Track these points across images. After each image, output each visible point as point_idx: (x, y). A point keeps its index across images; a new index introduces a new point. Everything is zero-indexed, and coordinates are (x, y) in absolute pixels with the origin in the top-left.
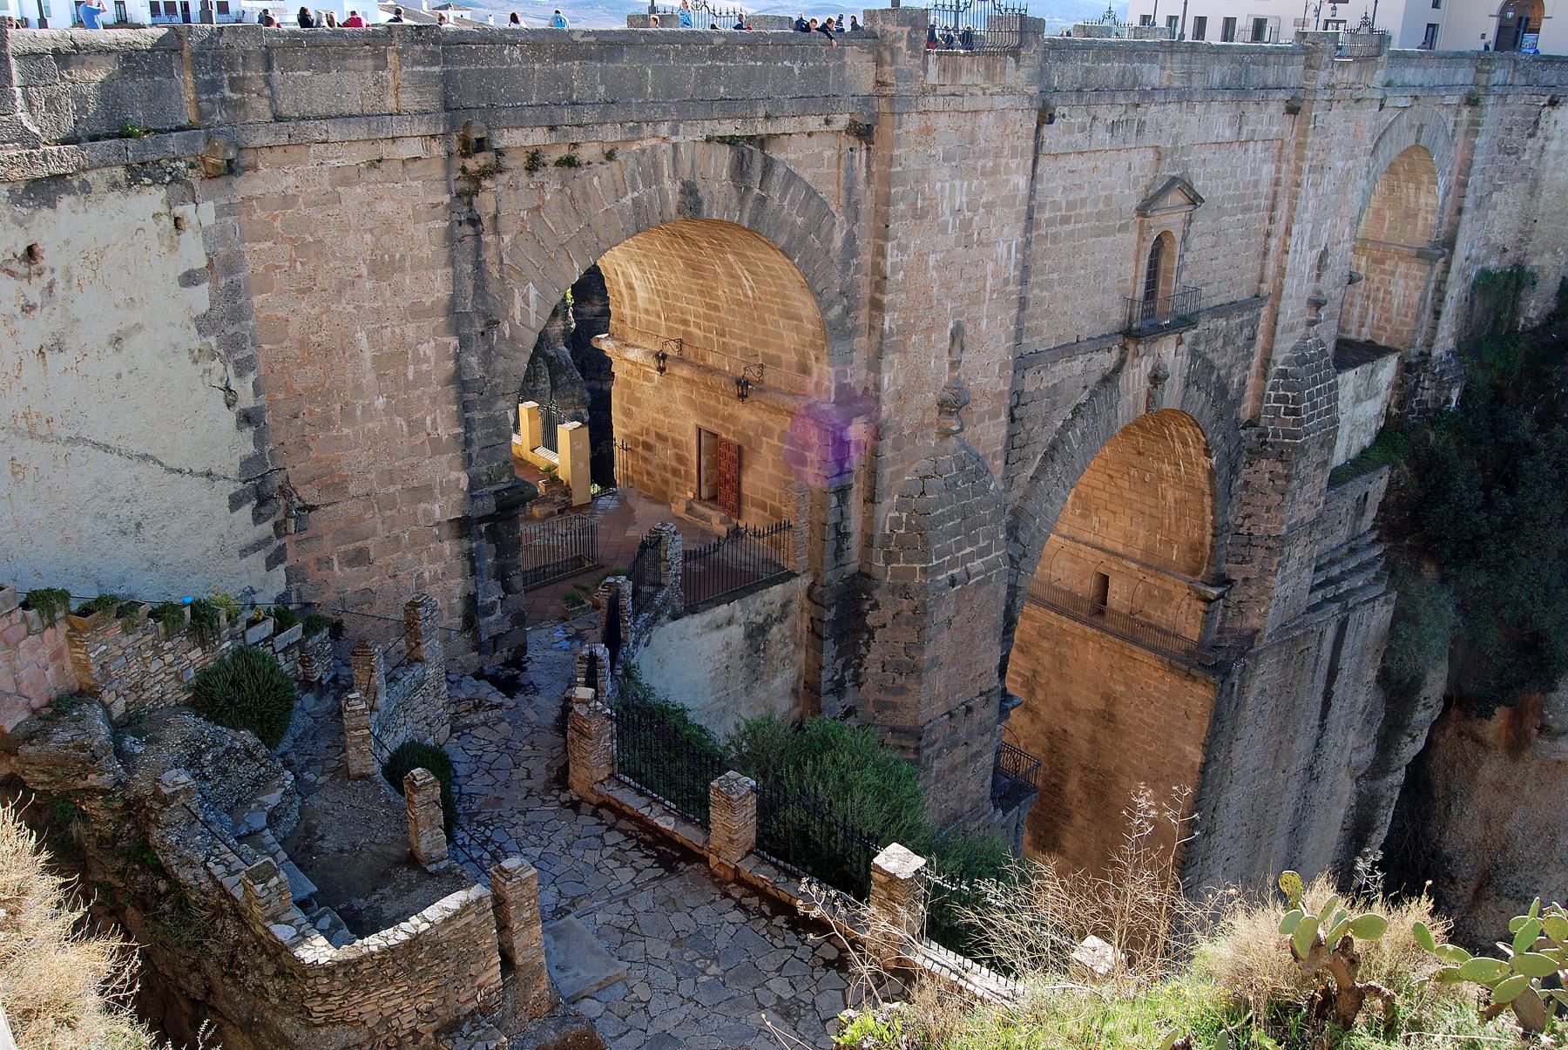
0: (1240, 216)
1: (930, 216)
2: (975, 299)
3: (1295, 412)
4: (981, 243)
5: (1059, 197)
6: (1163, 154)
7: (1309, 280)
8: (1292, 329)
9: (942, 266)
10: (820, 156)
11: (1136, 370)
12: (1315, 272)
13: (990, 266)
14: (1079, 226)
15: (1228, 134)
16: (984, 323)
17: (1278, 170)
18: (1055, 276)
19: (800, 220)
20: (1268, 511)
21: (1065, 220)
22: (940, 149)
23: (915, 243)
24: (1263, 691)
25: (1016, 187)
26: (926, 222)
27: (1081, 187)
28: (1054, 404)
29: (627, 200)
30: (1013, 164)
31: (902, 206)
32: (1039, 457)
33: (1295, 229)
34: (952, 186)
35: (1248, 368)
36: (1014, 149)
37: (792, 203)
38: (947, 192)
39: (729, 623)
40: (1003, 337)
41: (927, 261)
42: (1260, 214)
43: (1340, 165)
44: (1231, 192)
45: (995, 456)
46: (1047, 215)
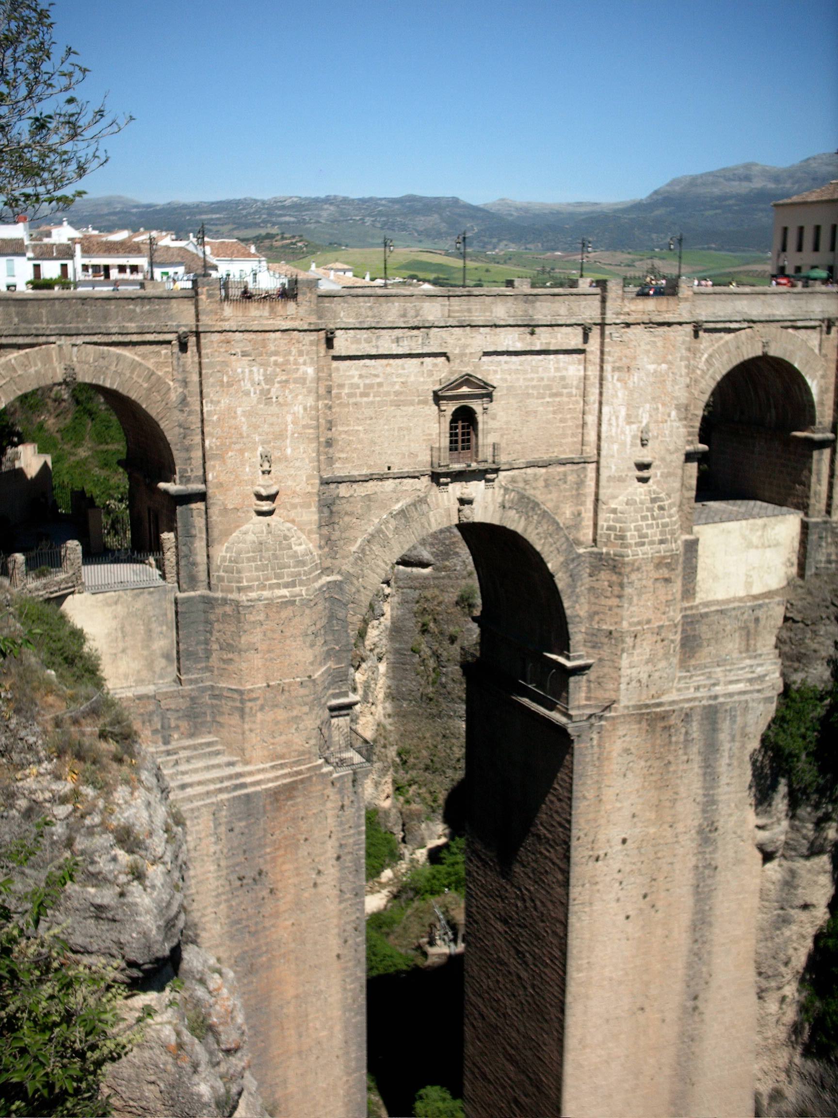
0: (548, 399)
1: (235, 387)
2: (280, 436)
3: (622, 538)
4: (279, 404)
5: (356, 380)
6: (451, 358)
7: (633, 445)
8: (621, 480)
9: (248, 414)
10: (158, 353)
11: (445, 494)
12: (639, 442)
13: (289, 418)
14: (378, 399)
15: (519, 347)
16: (289, 451)
17: (585, 369)
18: (360, 428)
19: (145, 385)
20: (610, 610)
21: (364, 395)
22: (238, 350)
23: (225, 402)
24: (627, 751)
25: (305, 373)
26: (232, 390)
27: (376, 376)
28: (369, 507)
29: (32, 370)
30: (301, 360)
31: (211, 380)
32: (359, 541)
33: (605, 409)
34: (251, 371)
35: (583, 504)
36: (301, 353)
37: (139, 376)
38: (247, 374)
39: (116, 603)
40: (307, 461)
41: (235, 413)
42: (574, 399)
43: (652, 367)
44: (534, 383)
45: (310, 532)
46: (346, 391)
